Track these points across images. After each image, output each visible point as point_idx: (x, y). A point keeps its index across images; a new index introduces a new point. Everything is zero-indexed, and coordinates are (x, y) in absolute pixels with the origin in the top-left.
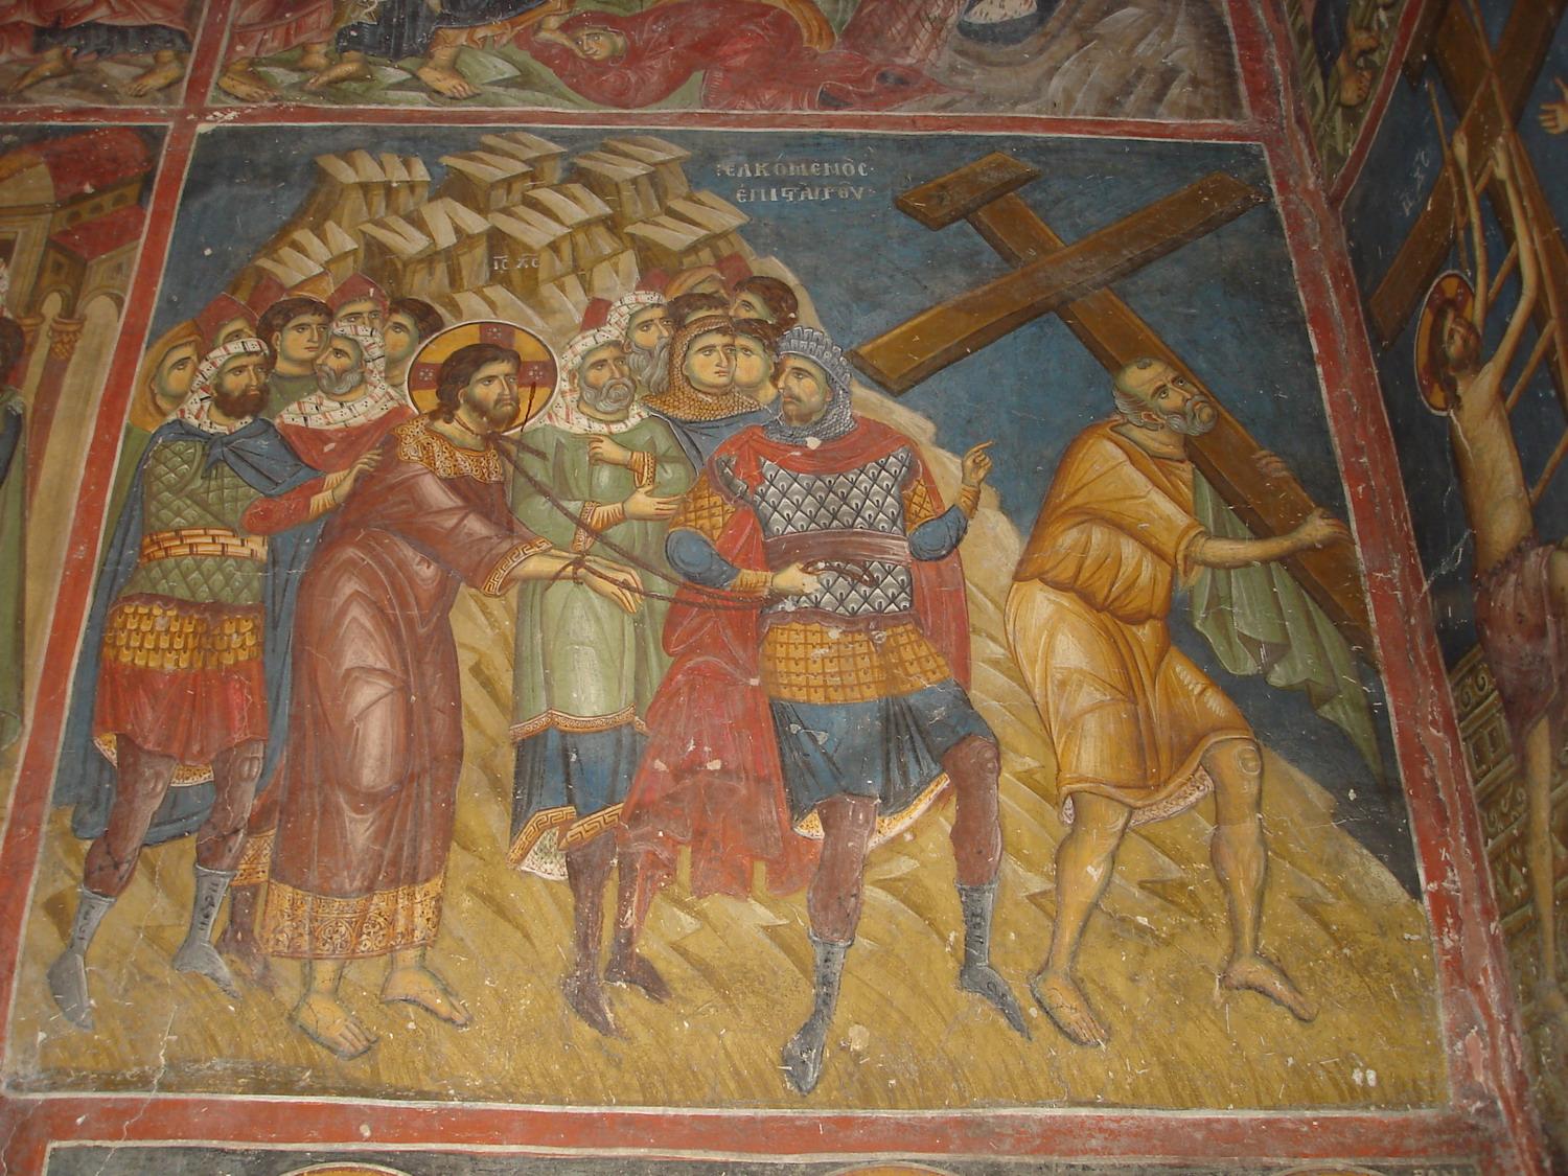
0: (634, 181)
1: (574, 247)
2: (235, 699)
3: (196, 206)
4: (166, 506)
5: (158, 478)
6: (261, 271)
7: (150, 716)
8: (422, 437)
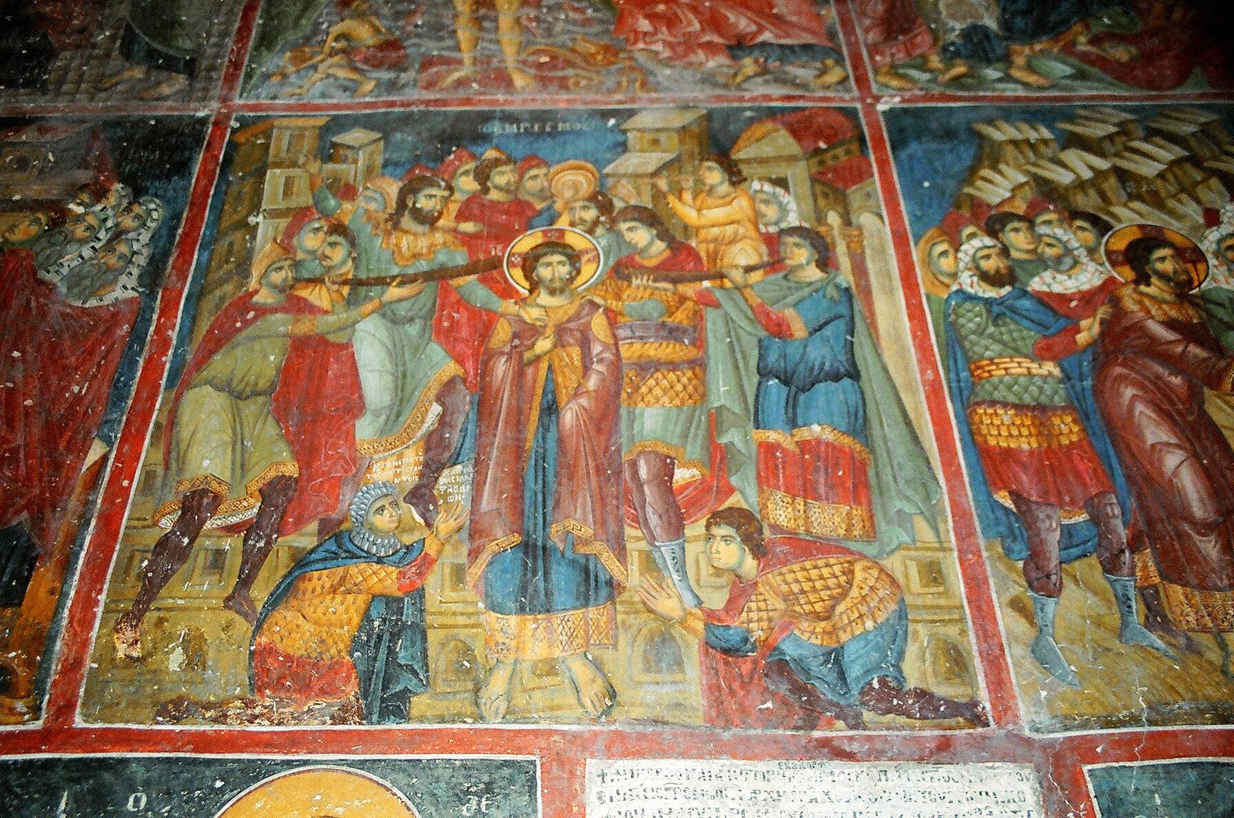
0: (1193, 134)
1: (1176, 177)
2: (1081, 466)
3: (903, 155)
4: (974, 344)
5: (963, 326)
6: (970, 196)
7: (1025, 478)
8: (1135, 296)
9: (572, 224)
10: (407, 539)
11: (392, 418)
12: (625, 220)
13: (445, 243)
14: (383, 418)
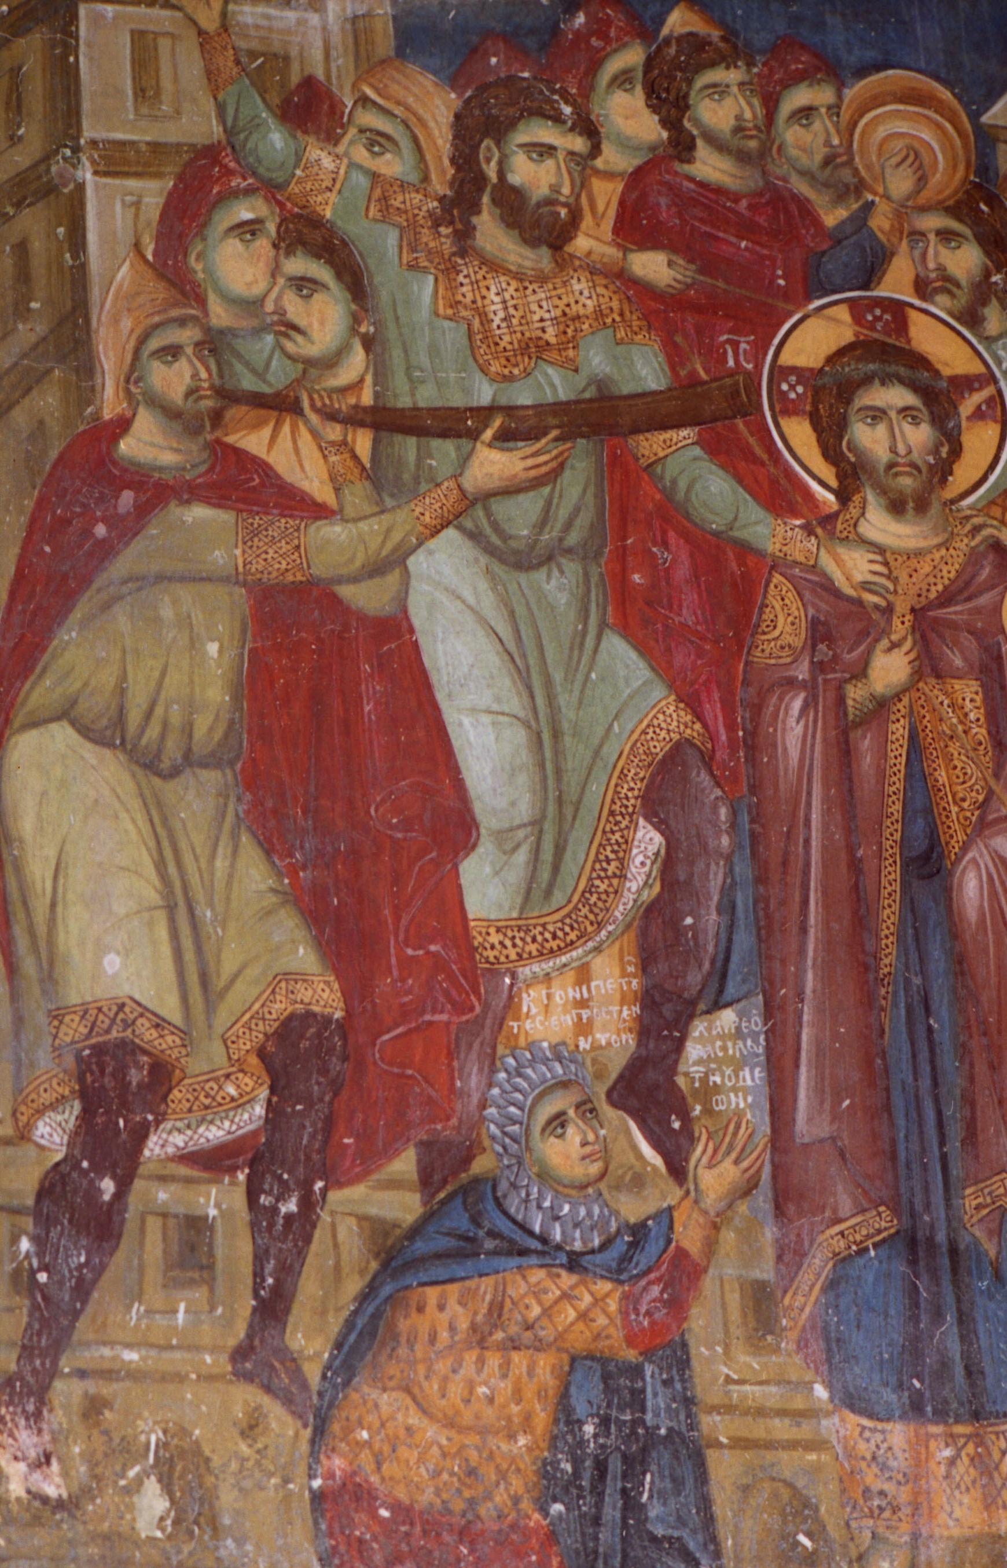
9: (922, 287)
10: (632, 1209)
11: (547, 854)
13: (599, 314)
14: (522, 857)
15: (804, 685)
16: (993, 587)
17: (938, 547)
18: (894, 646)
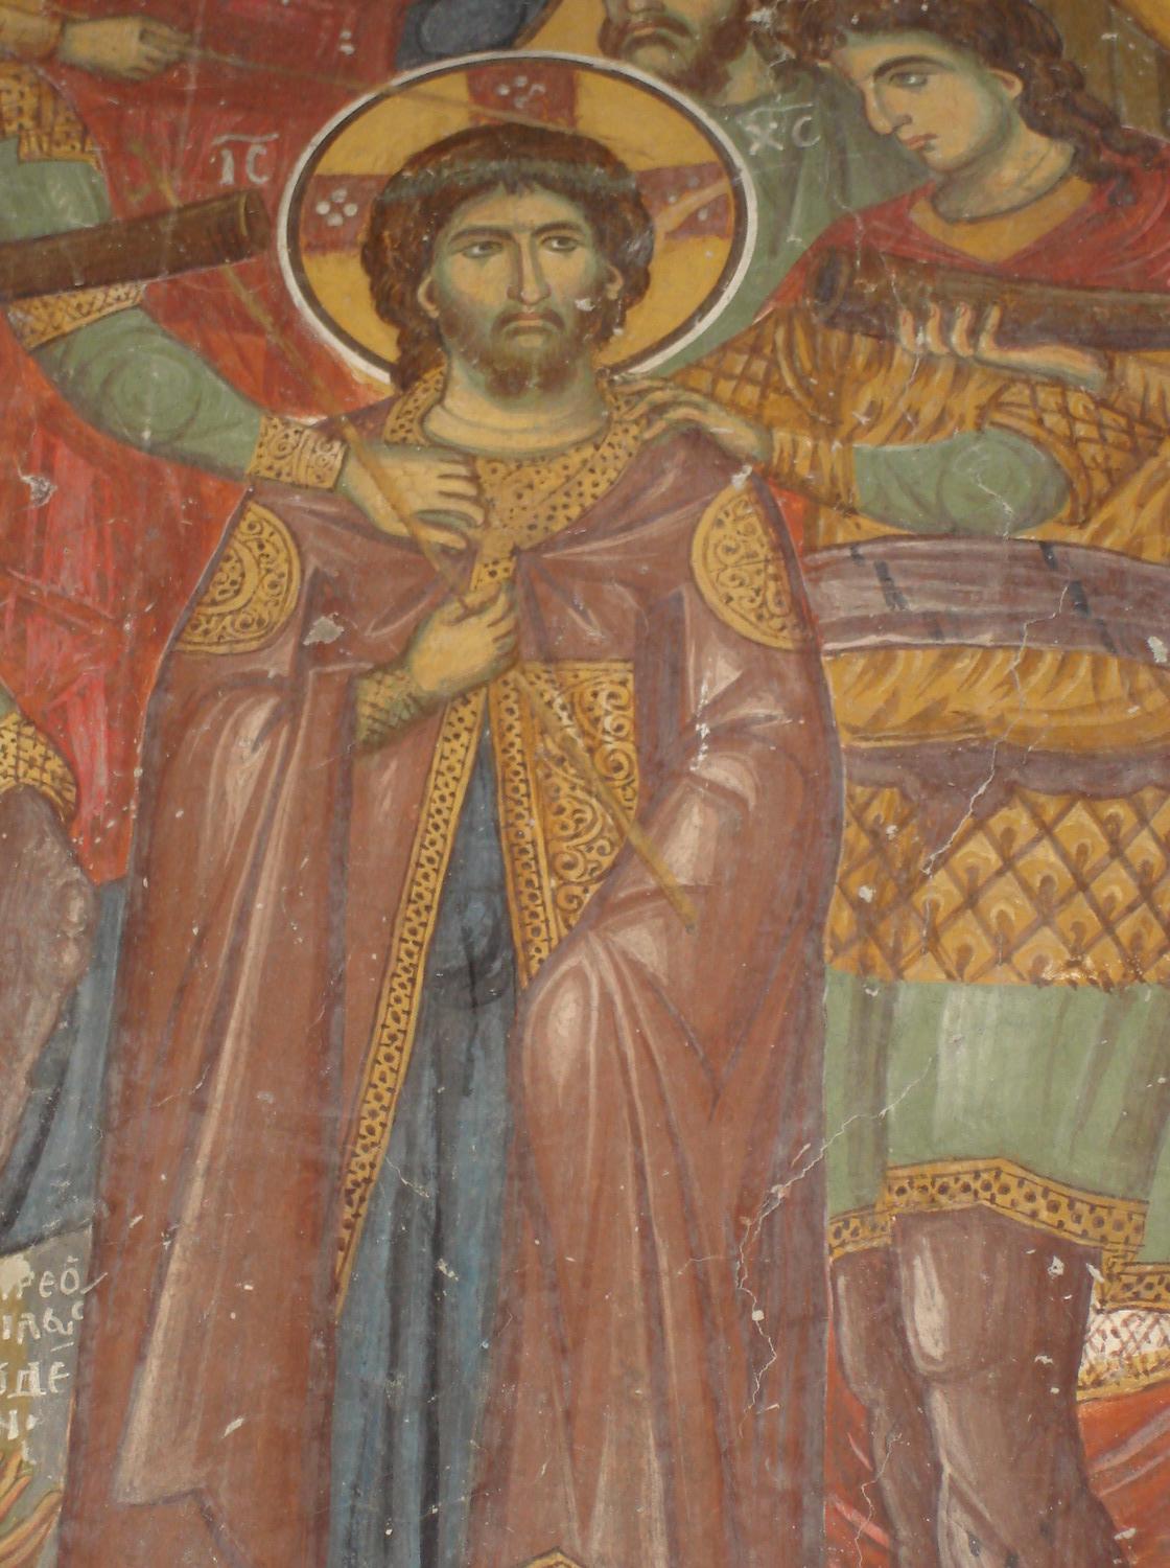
12: (867, 27)
15: (278, 686)
16: (687, 502)
17: (578, 445)
18: (470, 612)
